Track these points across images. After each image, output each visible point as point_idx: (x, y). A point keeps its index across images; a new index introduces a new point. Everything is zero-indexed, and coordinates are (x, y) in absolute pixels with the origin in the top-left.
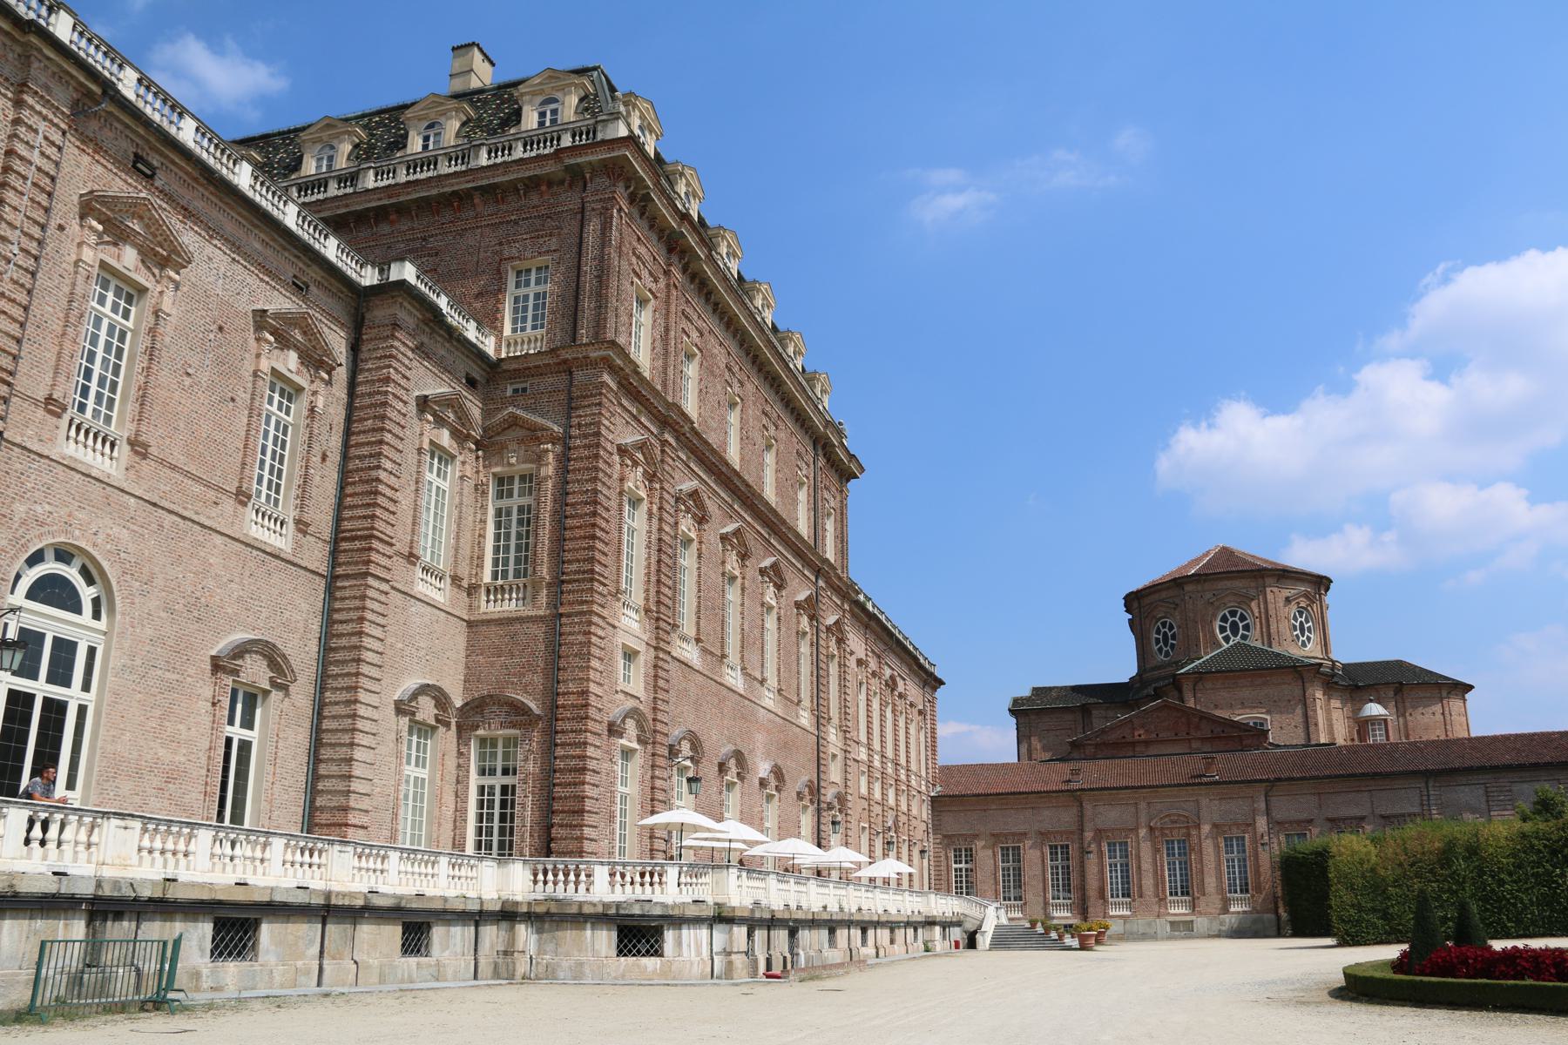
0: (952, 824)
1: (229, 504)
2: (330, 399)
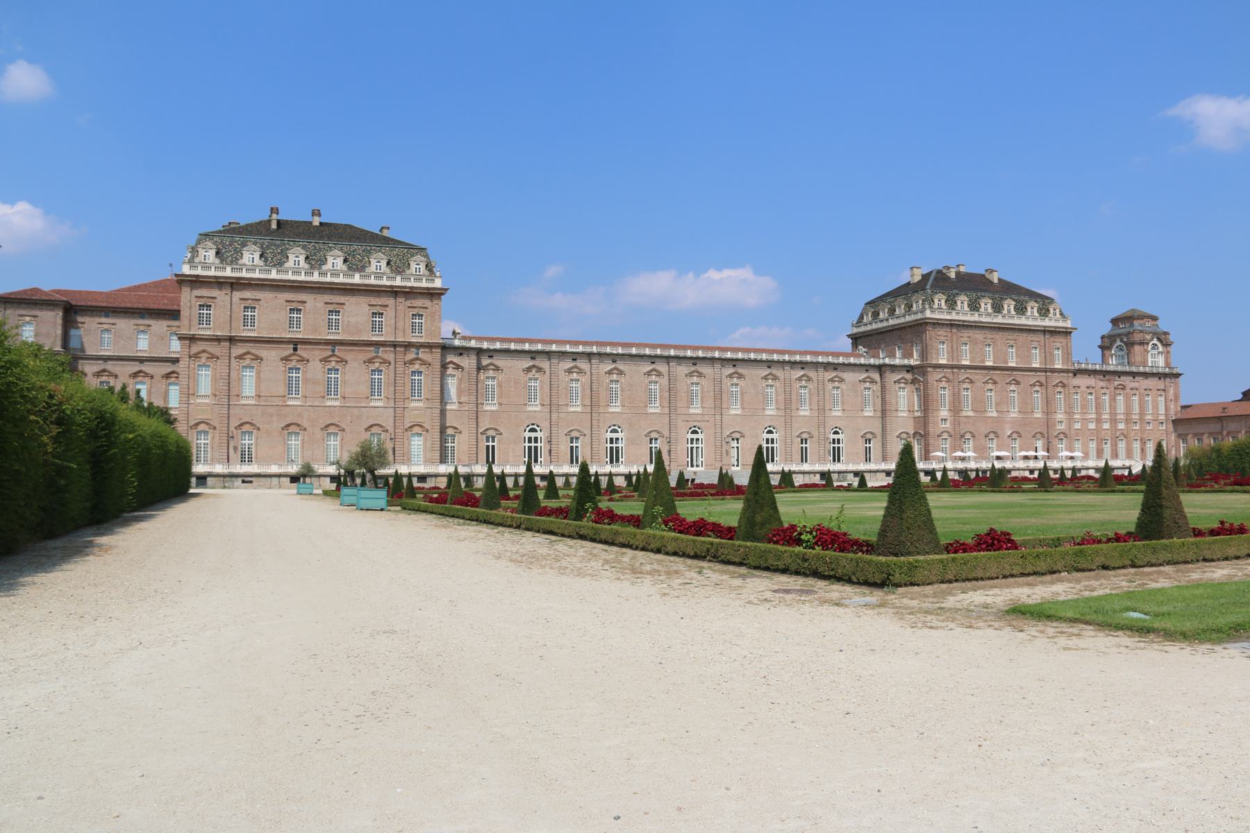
0: (1181, 430)
1: (860, 412)
2: (877, 387)
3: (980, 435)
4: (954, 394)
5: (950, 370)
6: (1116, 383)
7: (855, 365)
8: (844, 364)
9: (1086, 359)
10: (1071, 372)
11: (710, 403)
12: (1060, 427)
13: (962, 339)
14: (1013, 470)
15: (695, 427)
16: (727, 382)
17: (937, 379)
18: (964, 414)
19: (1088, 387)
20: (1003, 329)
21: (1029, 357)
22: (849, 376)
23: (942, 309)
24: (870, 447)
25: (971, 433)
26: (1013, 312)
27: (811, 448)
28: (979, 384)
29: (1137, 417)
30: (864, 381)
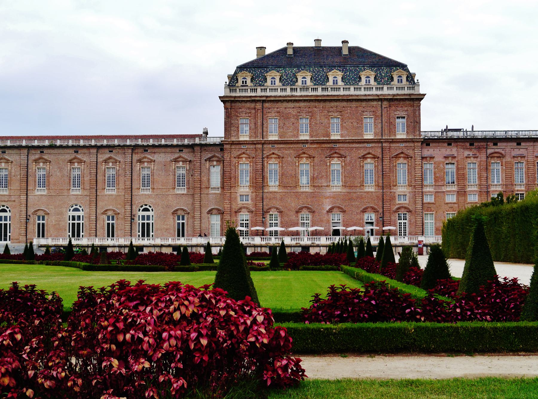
1: (171, 190)
3: (289, 210)
4: (255, 171)
5: (252, 146)
6: (490, 151)
7: (166, 146)
8: (154, 146)
9: (473, 127)
10: (418, 142)
11: (15, 185)
12: (400, 202)
13: (269, 115)
14: (311, 246)
15: (3, 206)
16: (33, 167)
17: (235, 156)
18: (272, 189)
19: (445, 157)
20: (325, 101)
21: (392, 127)
22: (160, 157)
23: (247, 86)
24: (183, 224)
25: (277, 209)
26: (340, 83)
27: (117, 224)
28: (289, 159)
29: (523, 188)
30: (176, 160)
